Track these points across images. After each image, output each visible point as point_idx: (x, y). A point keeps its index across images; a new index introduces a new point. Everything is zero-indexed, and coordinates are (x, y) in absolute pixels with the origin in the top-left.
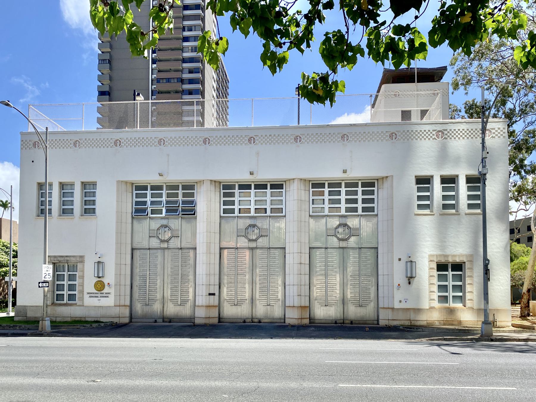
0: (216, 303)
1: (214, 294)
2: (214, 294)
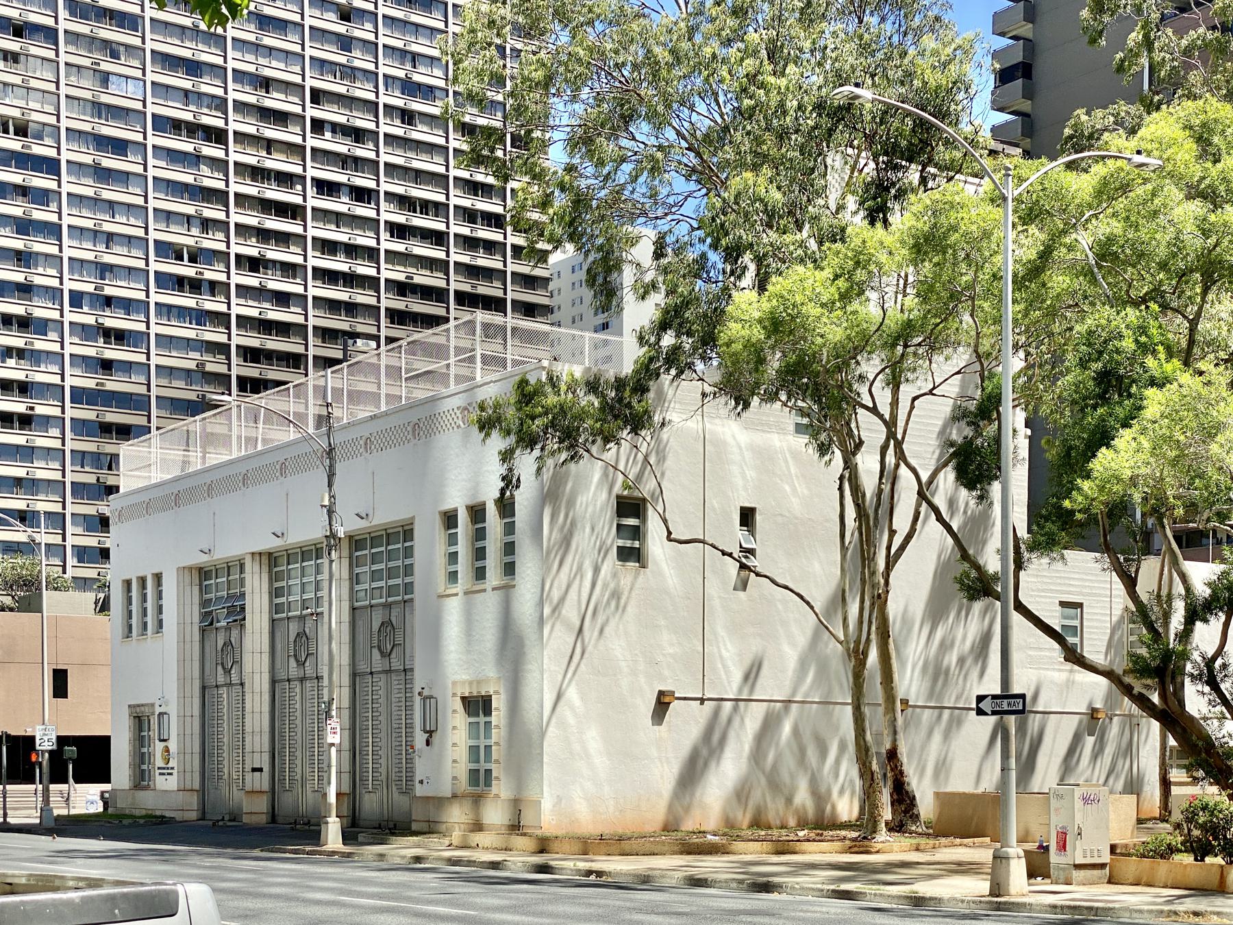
0: (266, 786)
1: (260, 770)
2: (260, 770)
